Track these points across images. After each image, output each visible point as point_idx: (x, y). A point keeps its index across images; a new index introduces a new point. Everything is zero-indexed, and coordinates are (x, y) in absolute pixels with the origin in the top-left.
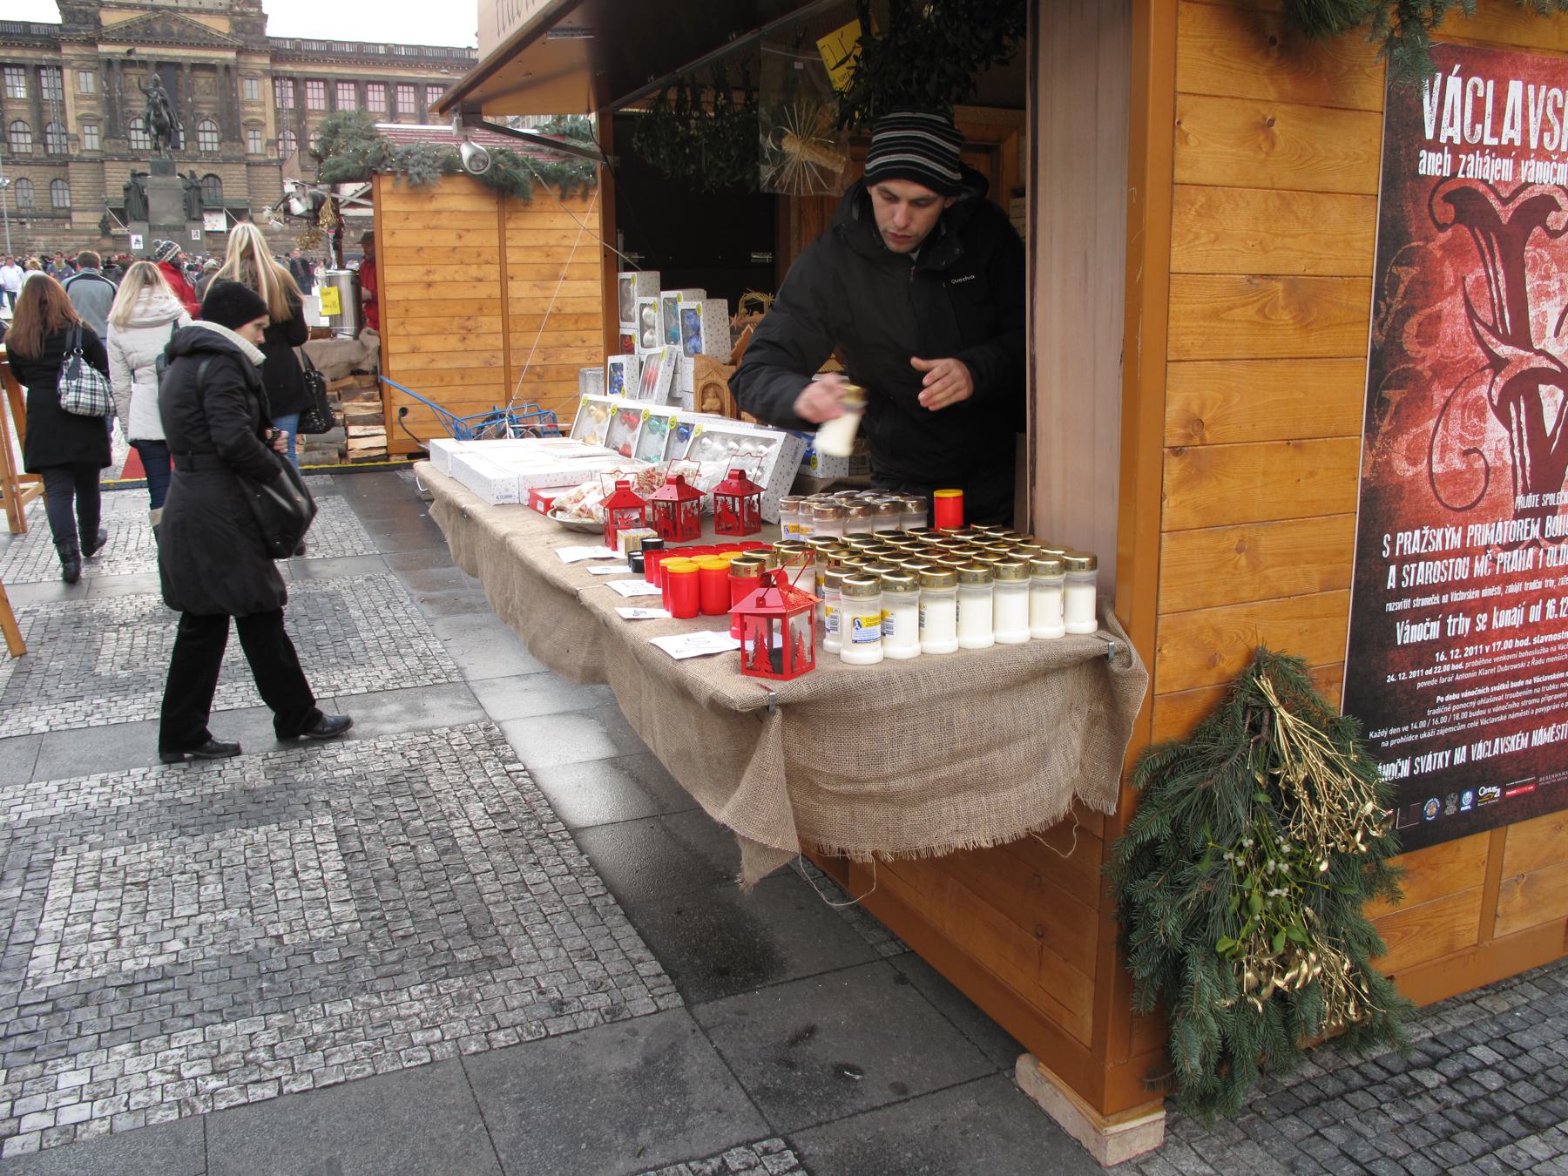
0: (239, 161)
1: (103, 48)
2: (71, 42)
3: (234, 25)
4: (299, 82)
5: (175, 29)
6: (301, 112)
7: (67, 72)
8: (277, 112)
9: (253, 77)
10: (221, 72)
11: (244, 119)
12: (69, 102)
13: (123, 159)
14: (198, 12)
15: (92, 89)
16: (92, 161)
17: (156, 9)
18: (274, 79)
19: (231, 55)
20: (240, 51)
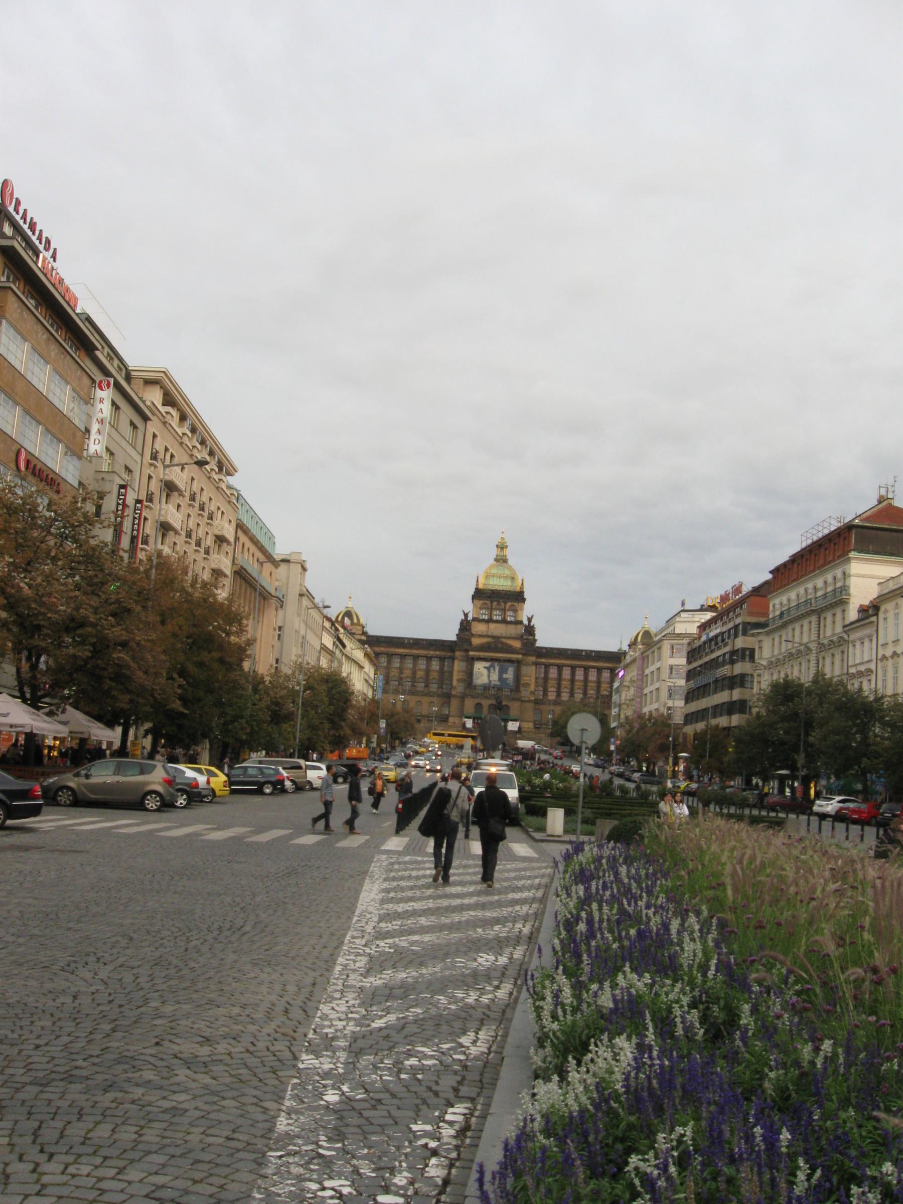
0: (518, 700)
1: (471, 653)
2: (460, 650)
3: (524, 645)
4: (547, 666)
5: (500, 646)
6: (546, 679)
7: (456, 662)
8: (536, 678)
9: (528, 665)
11: (522, 682)
12: (455, 673)
13: (472, 697)
14: (509, 638)
15: (464, 668)
16: (460, 697)
17: (493, 637)
19: (520, 656)
20: (524, 655)
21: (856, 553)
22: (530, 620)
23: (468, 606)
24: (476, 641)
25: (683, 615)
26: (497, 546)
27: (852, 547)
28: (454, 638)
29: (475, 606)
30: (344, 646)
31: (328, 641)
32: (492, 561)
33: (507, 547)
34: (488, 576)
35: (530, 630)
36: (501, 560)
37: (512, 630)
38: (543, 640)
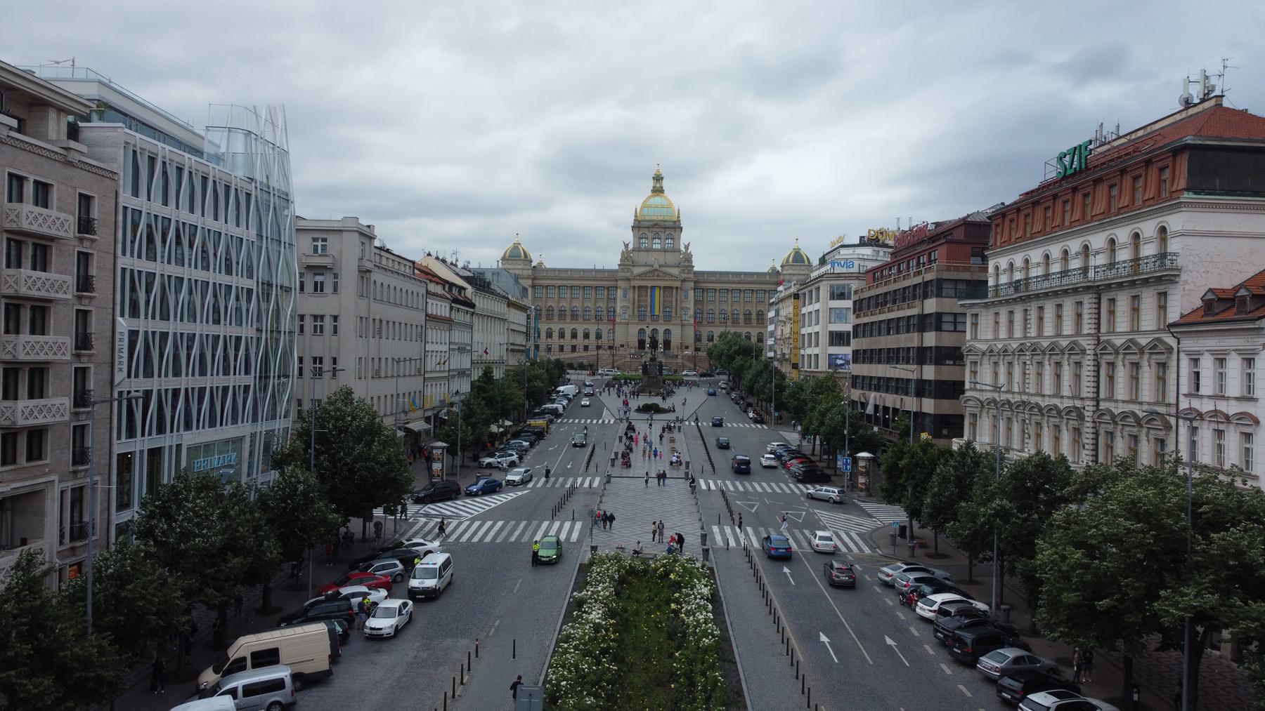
7: (619, 290)
10: (674, 291)
18: (695, 289)
21: (1191, 195)
22: (687, 247)
23: (629, 236)
24: (637, 271)
25: (843, 251)
26: (654, 178)
27: (1182, 184)
28: (617, 267)
29: (634, 237)
30: (472, 306)
31: (440, 308)
32: (650, 193)
33: (662, 178)
34: (644, 206)
35: (688, 258)
36: (658, 191)
37: (671, 258)
38: (698, 267)
